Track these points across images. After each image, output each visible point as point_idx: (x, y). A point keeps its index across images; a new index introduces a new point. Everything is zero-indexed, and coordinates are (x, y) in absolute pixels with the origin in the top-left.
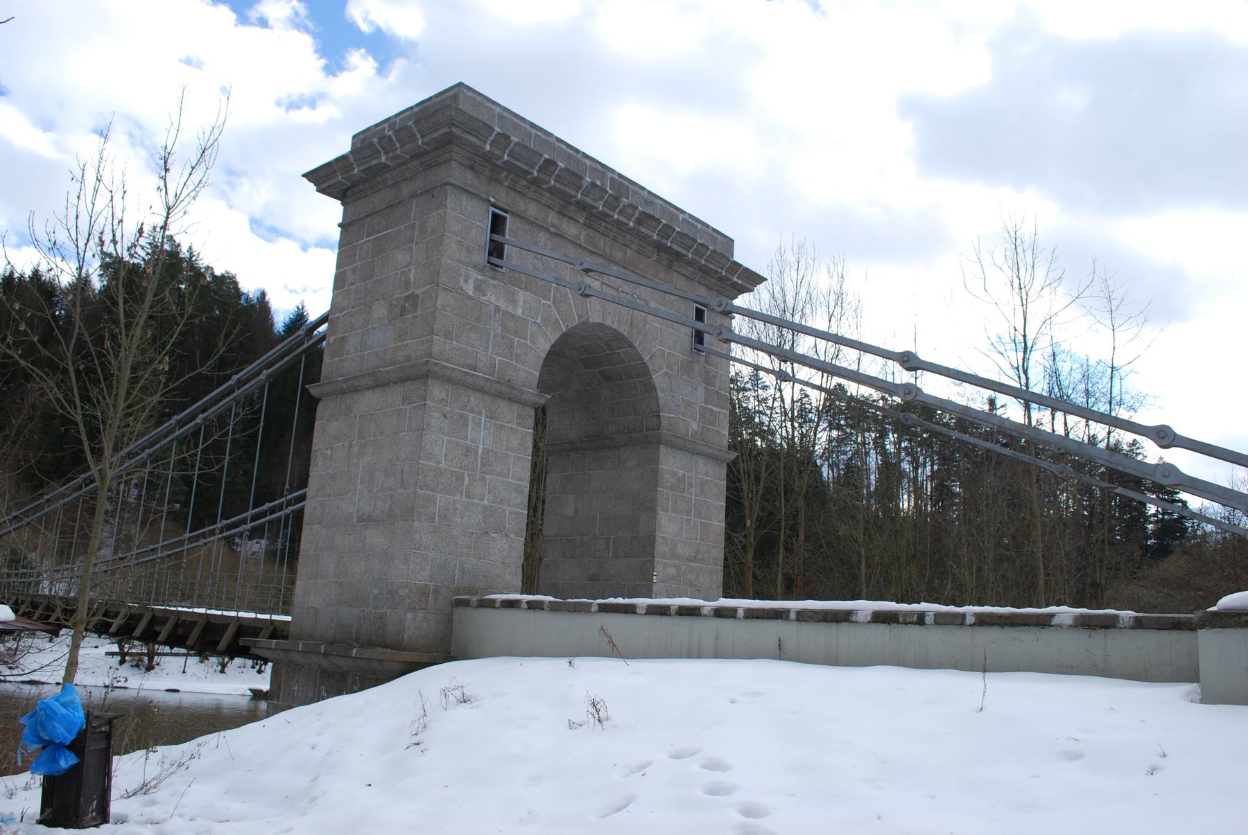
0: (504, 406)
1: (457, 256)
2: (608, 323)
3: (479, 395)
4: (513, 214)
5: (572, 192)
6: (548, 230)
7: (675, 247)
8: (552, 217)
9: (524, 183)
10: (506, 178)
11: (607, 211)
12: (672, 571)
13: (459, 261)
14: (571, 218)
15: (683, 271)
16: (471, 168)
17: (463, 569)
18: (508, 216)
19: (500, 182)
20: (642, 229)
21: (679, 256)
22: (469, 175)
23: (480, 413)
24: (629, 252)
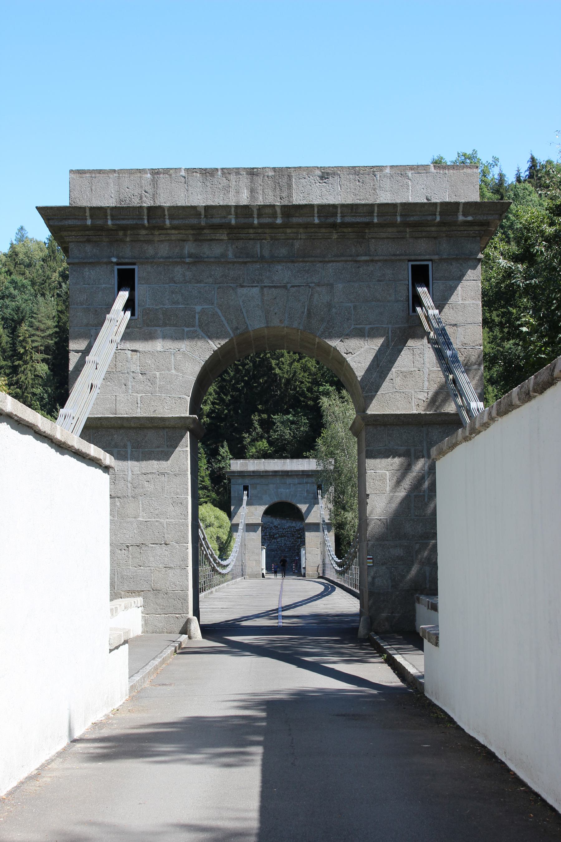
0: (150, 434)
1: (85, 321)
2: (275, 322)
3: (122, 431)
4: (142, 263)
5: (194, 221)
6: (184, 263)
7: (348, 219)
8: (189, 248)
9: (143, 232)
10: (125, 235)
11: (242, 221)
12: (399, 552)
13: (87, 325)
14: (217, 240)
15: (383, 235)
16: (89, 241)
17: (122, 577)
18: (135, 267)
19: (122, 241)
20: (295, 220)
21: (369, 225)
22: (88, 248)
23: (125, 446)
24: (297, 244)
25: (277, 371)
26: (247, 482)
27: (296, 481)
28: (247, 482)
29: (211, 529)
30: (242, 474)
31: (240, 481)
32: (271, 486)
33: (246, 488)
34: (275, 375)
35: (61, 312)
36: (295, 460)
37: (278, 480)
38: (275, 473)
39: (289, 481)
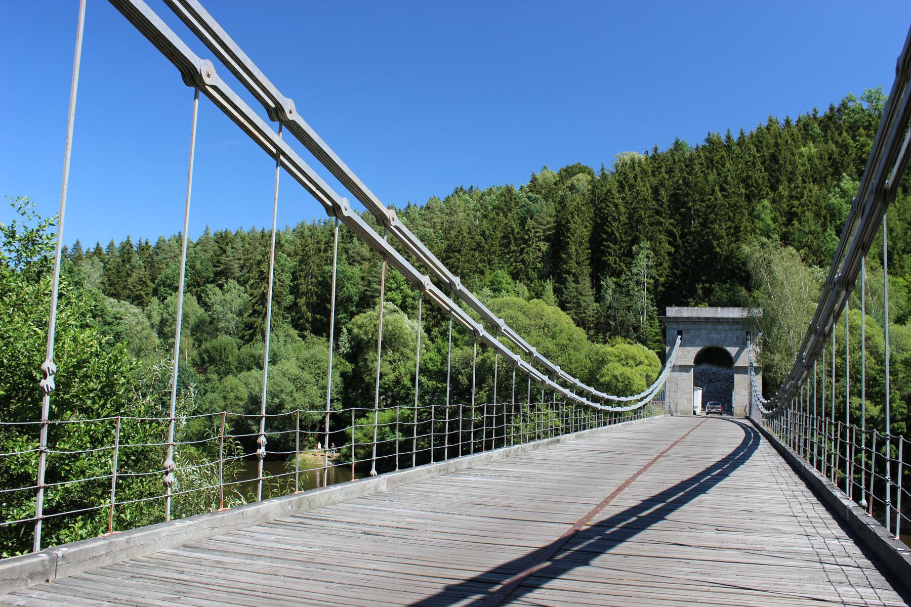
25: (718, 249)
26: (681, 327)
27: (727, 327)
28: (681, 327)
29: (640, 367)
30: (676, 320)
31: (675, 326)
32: (703, 332)
33: (680, 333)
34: (717, 253)
35: (559, 212)
36: (726, 309)
37: (710, 326)
38: (707, 320)
39: (720, 327)
